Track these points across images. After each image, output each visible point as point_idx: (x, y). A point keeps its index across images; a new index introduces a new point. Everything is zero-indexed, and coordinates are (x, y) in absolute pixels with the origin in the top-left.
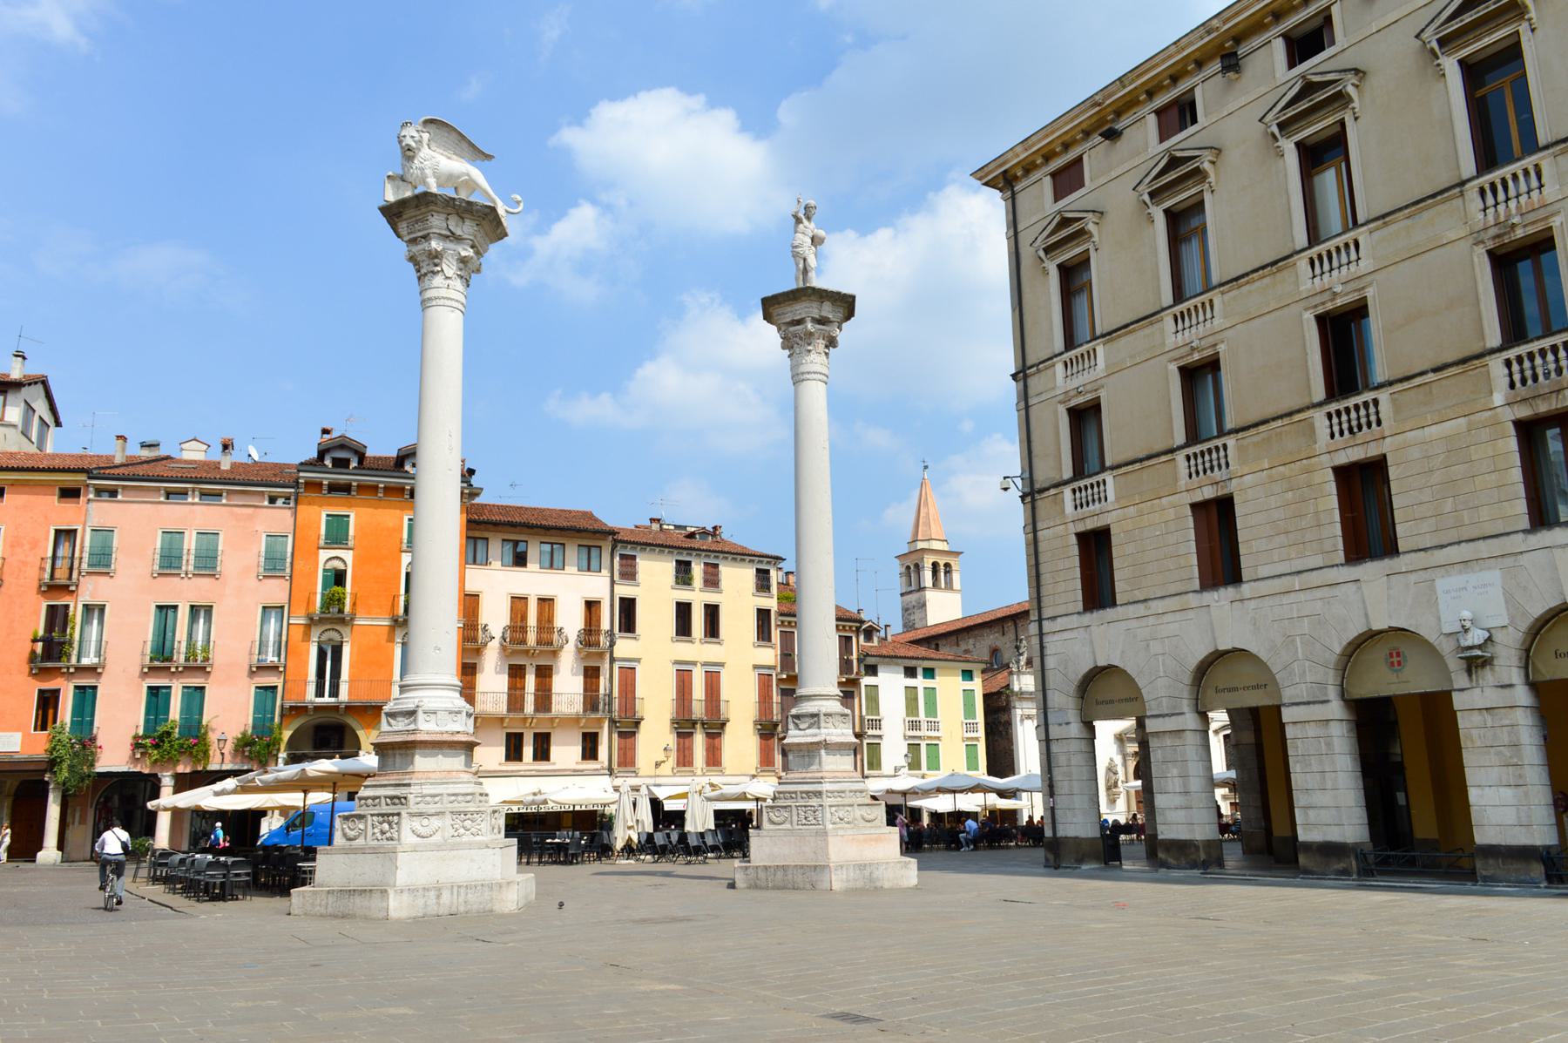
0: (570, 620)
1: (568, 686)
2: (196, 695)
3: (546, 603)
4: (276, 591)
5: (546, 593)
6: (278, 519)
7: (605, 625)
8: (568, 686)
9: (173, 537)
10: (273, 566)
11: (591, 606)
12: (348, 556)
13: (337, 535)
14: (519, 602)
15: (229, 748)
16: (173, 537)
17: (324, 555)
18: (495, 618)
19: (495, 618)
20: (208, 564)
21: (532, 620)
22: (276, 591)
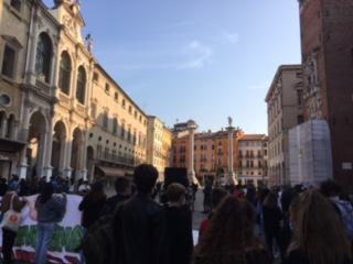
0: (256, 153)
1: (256, 163)
4: (213, 152)
6: (212, 143)
8: (256, 163)
11: (259, 152)
13: (220, 144)
18: (244, 154)
20: (202, 147)
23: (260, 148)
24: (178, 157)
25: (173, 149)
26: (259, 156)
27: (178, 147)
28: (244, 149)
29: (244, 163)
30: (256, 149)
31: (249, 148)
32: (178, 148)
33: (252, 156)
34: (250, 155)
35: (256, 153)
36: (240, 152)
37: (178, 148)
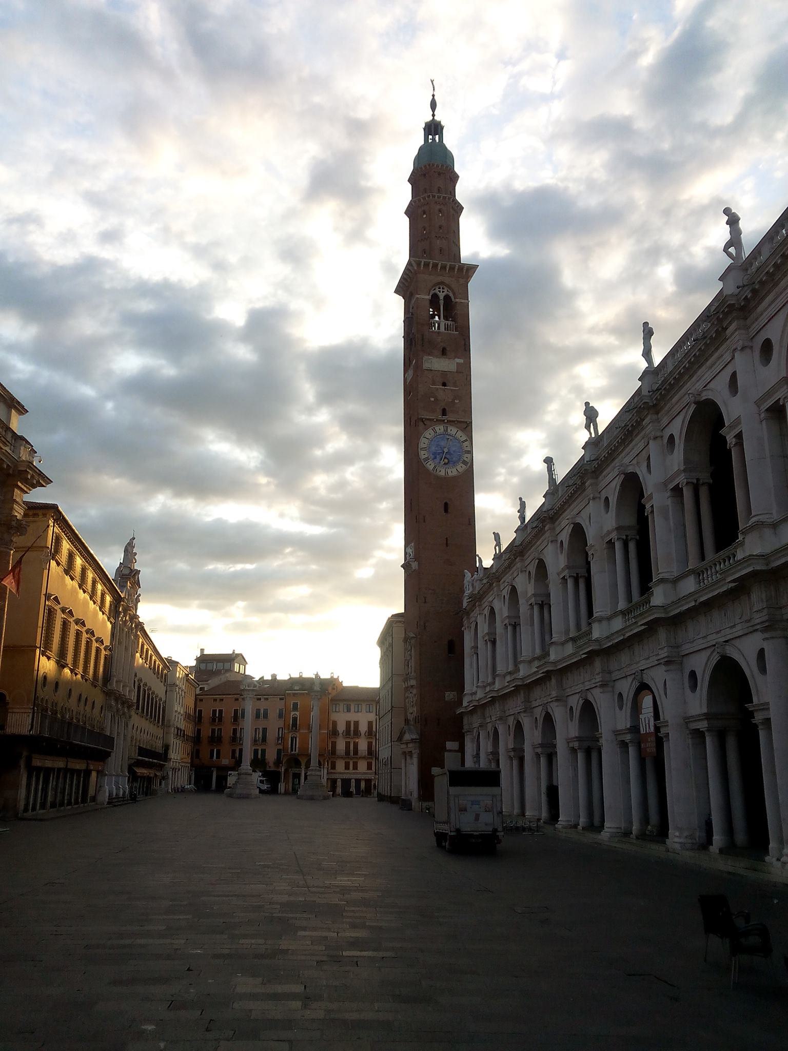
0: (363, 728)
1: (363, 746)
2: (264, 751)
3: (356, 724)
5: (356, 720)
7: (374, 729)
9: (258, 711)
10: (280, 716)
11: (370, 723)
12: (298, 713)
14: (348, 724)
15: (271, 764)
16: (258, 711)
17: (292, 713)
18: (341, 728)
19: (341, 728)
20: (266, 715)
21: (352, 728)
22: (281, 723)
23: (372, 717)
24: (206, 732)
25: (197, 718)
26: (370, 733)
27: (207, 710)
28: (341, 719)
29: (341, 746)
30: (364, 718)
31: (352, 717)
32: (207, 714)
33: (357, 733)
34: (352, 730)
35: (363, 728)
36: (335, 724)
37: (207, 714)
